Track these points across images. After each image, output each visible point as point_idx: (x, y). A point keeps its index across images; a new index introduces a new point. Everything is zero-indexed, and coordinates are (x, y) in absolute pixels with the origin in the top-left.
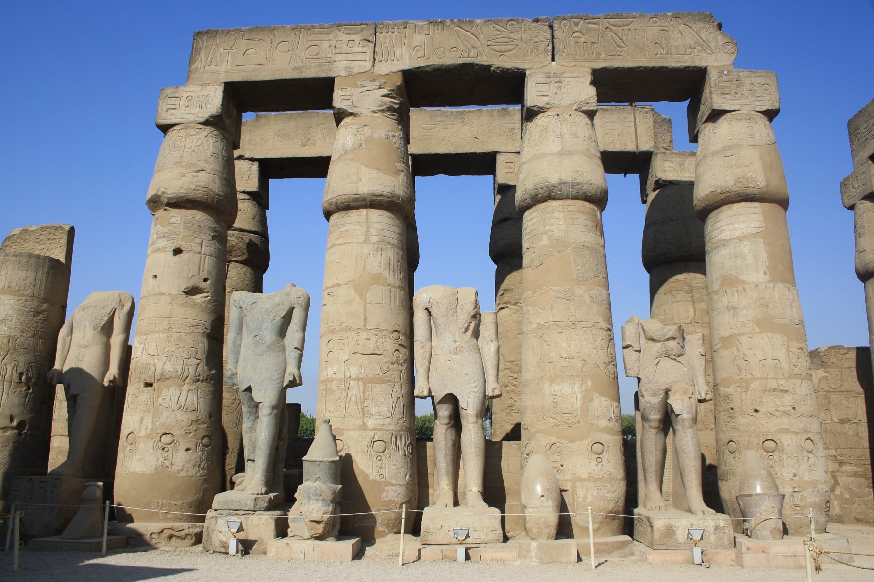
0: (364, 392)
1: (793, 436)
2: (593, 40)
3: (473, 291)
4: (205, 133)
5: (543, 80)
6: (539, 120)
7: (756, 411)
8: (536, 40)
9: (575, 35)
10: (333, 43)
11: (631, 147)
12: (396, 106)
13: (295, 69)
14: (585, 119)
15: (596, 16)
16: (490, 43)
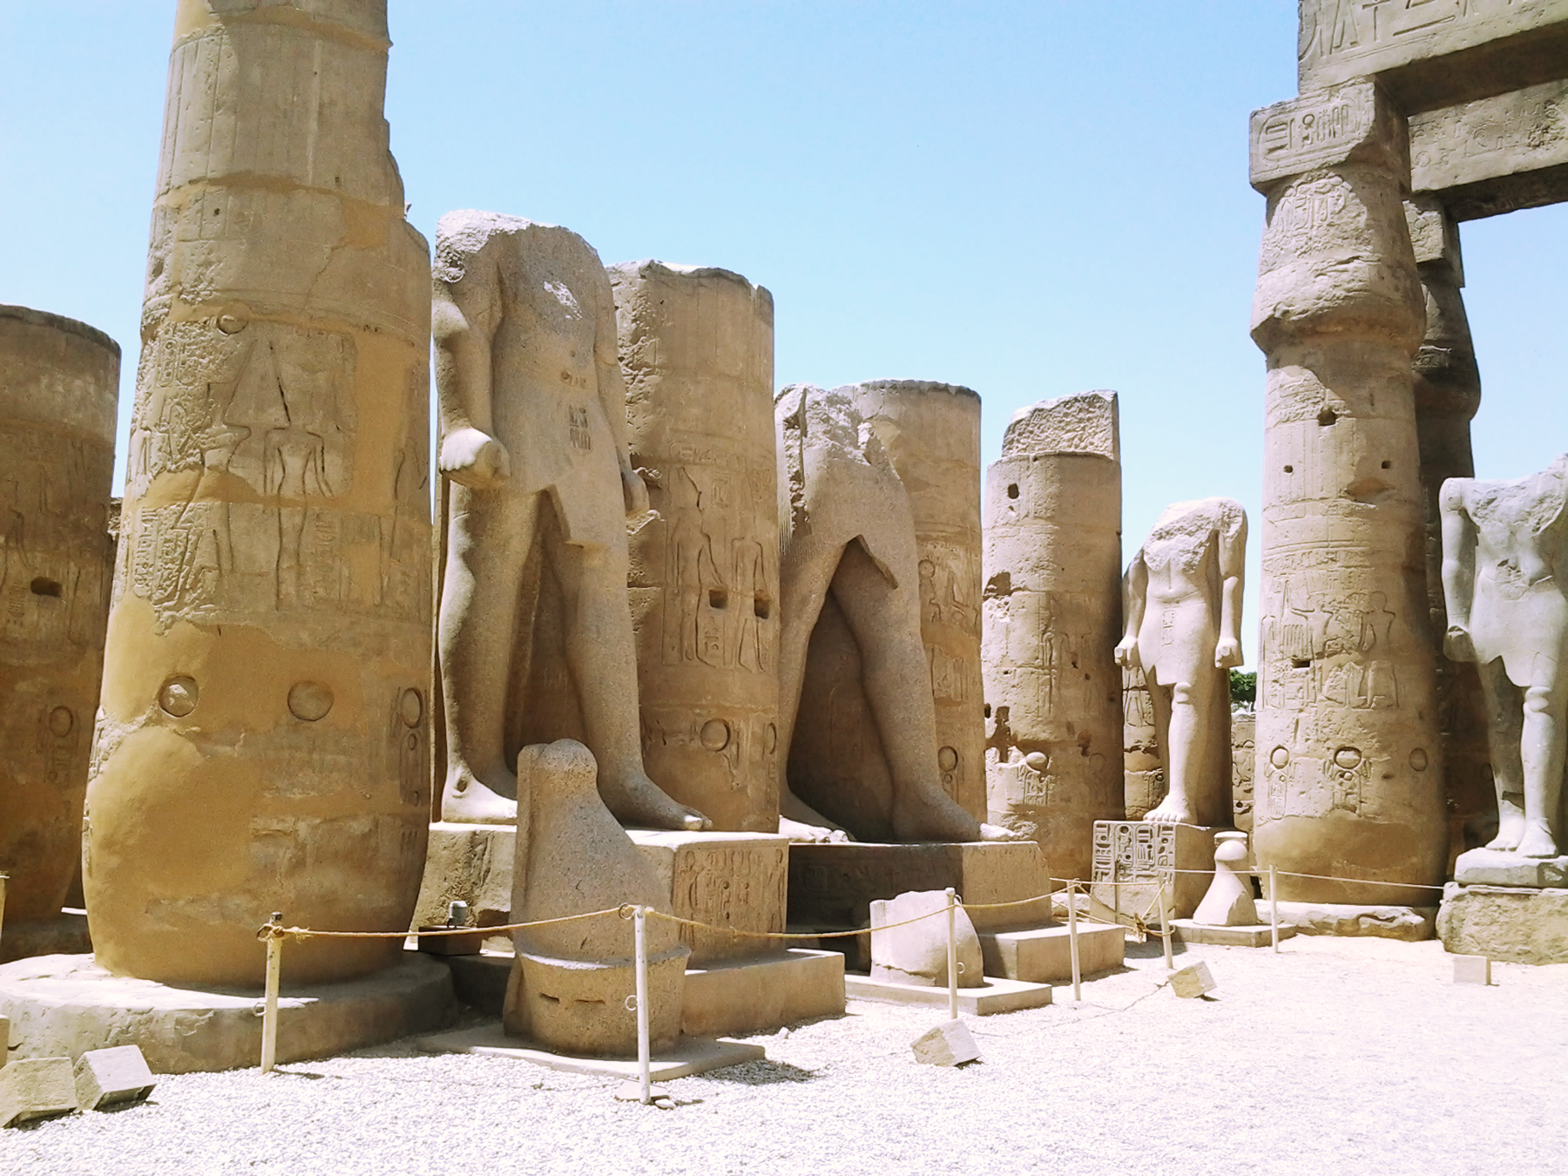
13: (1524, 10)
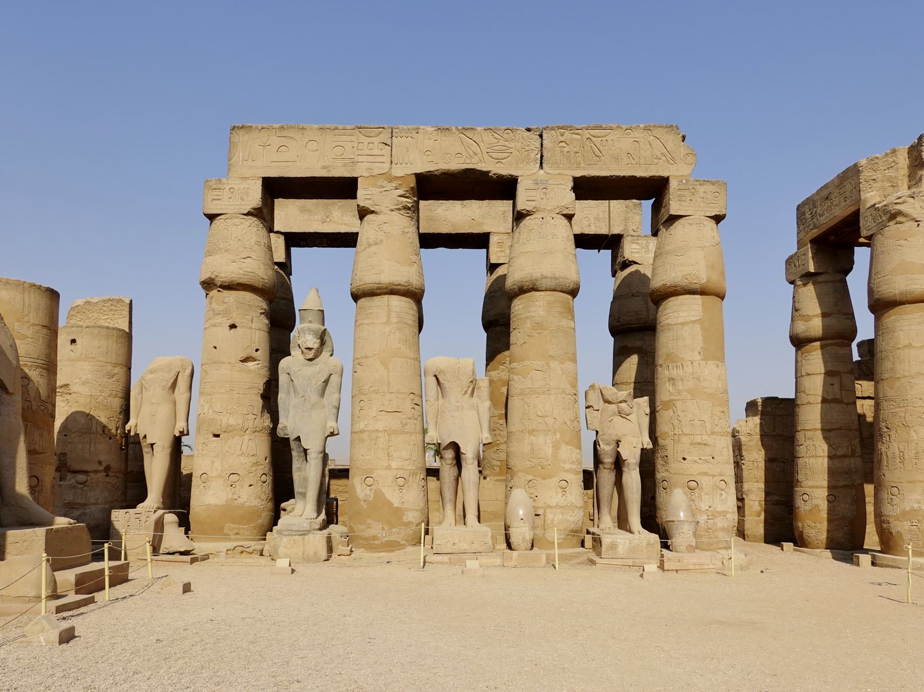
0: (389, 441)
1: (711, 478)
2: (575, 150)
3: (471, 361)
4: (248, 223)
5: (532, 187)
6: (527, 221)
7: (684, 459)
8: (527, 148)
9: (561, 144)
10: (355, 145)
11: (604, 231)
12: (410, 205)
13: (324, 167)
14: (565, 221)
15: (579, 127)
16: (489, 150)
